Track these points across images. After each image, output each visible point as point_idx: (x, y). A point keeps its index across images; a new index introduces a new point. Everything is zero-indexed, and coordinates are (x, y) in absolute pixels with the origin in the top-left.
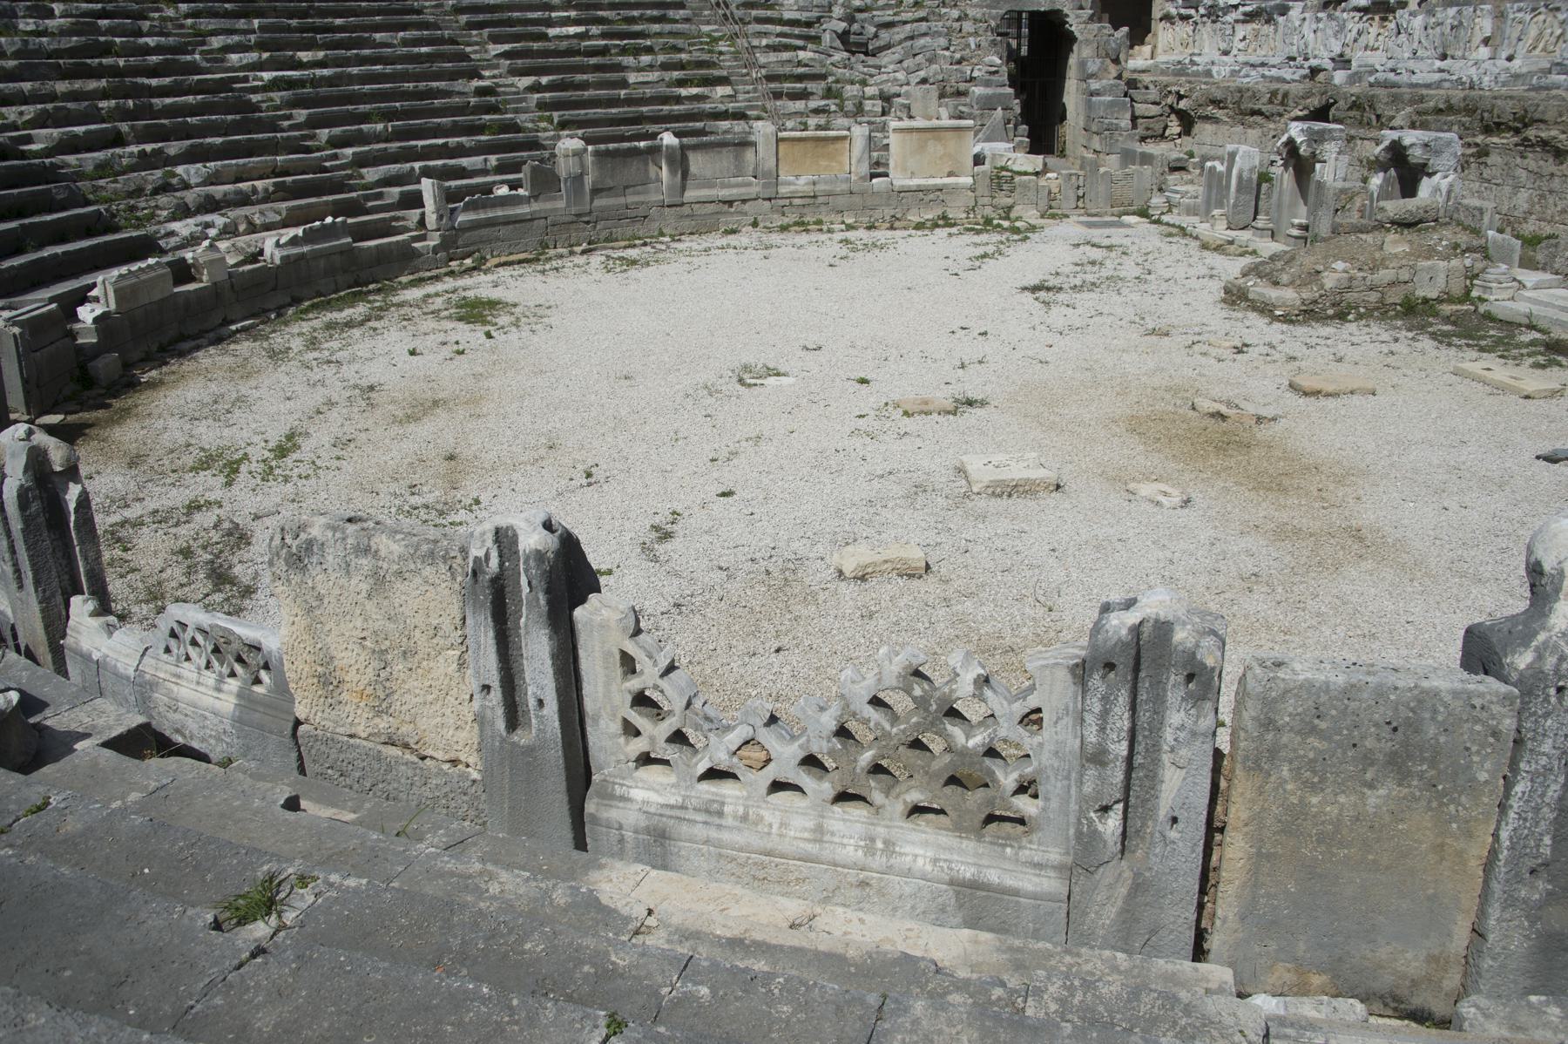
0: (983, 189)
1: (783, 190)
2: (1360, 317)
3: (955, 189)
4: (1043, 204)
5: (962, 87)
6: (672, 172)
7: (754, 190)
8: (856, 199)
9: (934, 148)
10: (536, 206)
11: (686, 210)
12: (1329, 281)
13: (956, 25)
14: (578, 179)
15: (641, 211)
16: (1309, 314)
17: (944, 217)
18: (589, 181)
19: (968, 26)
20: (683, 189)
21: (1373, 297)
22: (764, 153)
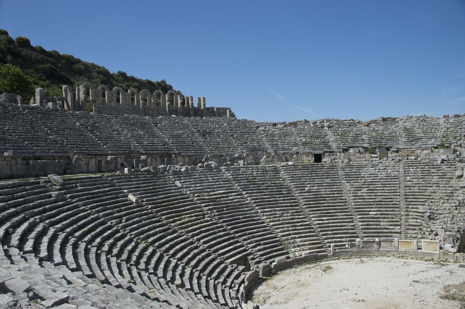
0: (441, 254)
1: (399, 250)
2: (458, 300)
3: (435, 254)
4: (455, 259)
5: (451, 230)
6: (377, 245)
7: (393, 250)
8: (414, 253)
9: (431, 245)
10: (351, 249)
11: (380, 252)
12: (451, 292)
13: (457, 215)
14: (359, 246)
15: (371, 251)
16: (446, 297)
17: (433, 259)
18: (361, 246)
19: (459, 215)
20: (379, 248)
21: (461, 297)
22: (395, 243)
